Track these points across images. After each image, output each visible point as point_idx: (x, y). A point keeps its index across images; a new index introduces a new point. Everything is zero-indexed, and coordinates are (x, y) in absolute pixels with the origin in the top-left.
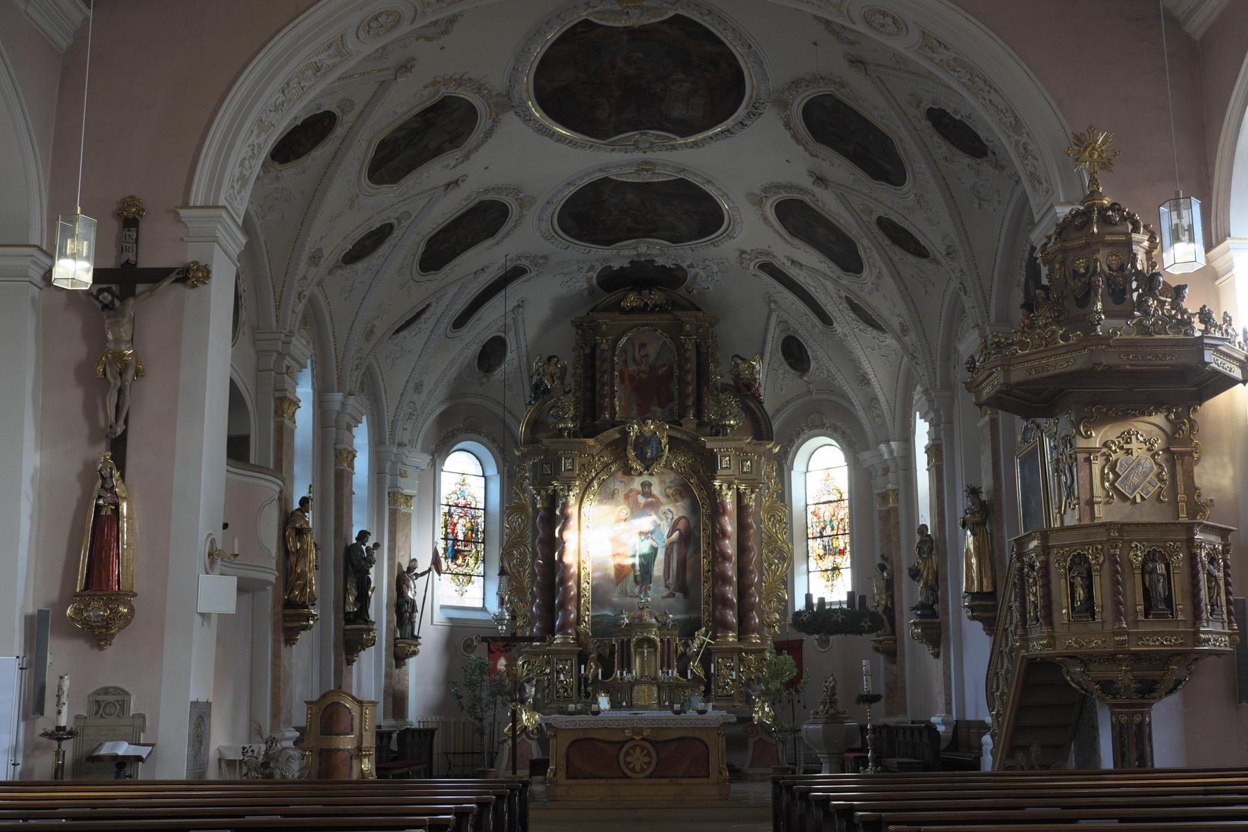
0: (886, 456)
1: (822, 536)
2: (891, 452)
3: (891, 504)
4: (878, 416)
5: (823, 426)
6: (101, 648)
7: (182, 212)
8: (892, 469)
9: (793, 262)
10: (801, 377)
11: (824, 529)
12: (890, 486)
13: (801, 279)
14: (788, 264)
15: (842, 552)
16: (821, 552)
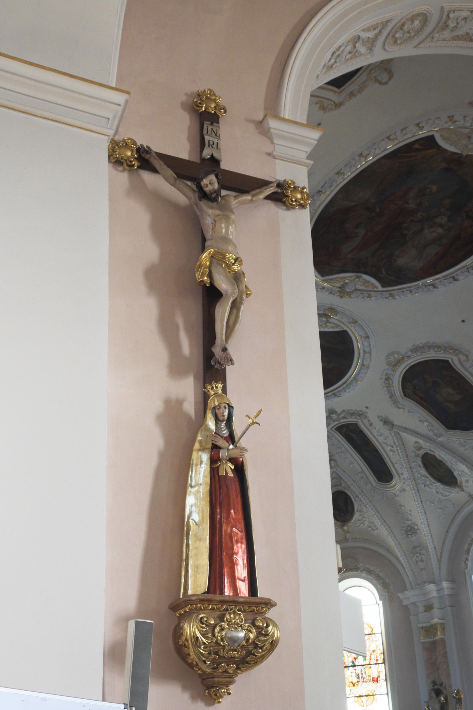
0: (435, 594)
1: (354, 666)
2: (440, 590)
3: (439, 635)
4: (422, 560)
5: (356, 569)
6: (213, 704)
7: (273, 124)
8: (436, 604)
9: (386, 422)
10: (342, 526)
11: (355, 659)
12: (436, 620)
13: (381, 439)
14: (379, 425)
15: (376, 680)
16: (355, 680)
